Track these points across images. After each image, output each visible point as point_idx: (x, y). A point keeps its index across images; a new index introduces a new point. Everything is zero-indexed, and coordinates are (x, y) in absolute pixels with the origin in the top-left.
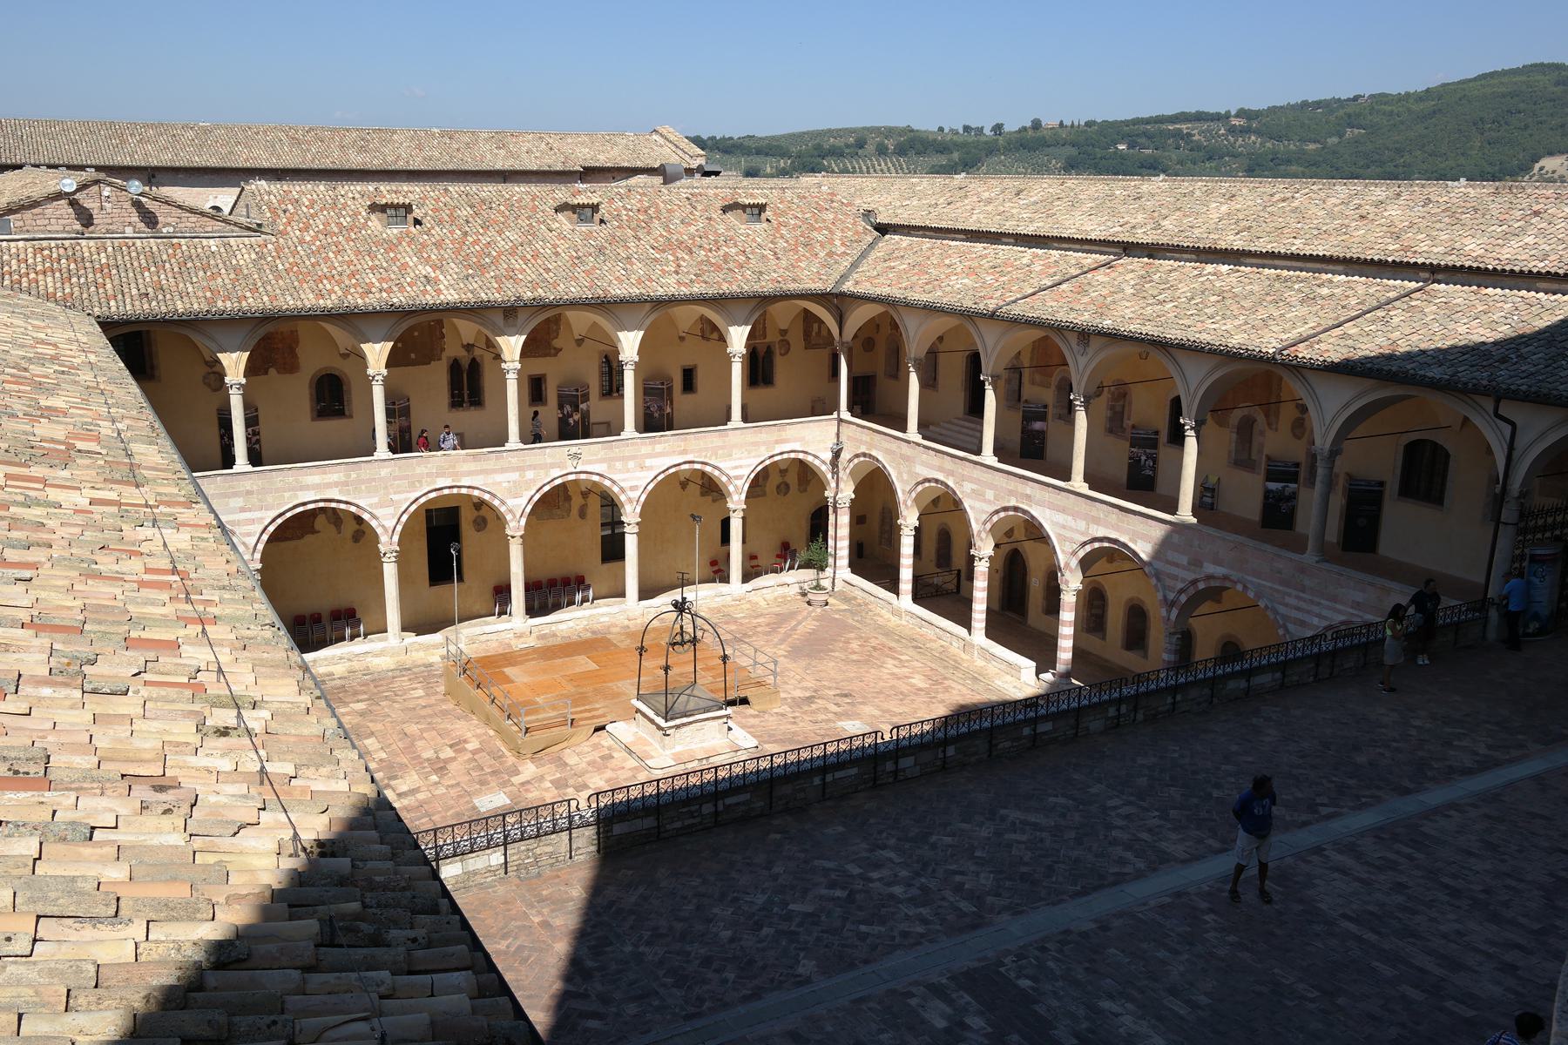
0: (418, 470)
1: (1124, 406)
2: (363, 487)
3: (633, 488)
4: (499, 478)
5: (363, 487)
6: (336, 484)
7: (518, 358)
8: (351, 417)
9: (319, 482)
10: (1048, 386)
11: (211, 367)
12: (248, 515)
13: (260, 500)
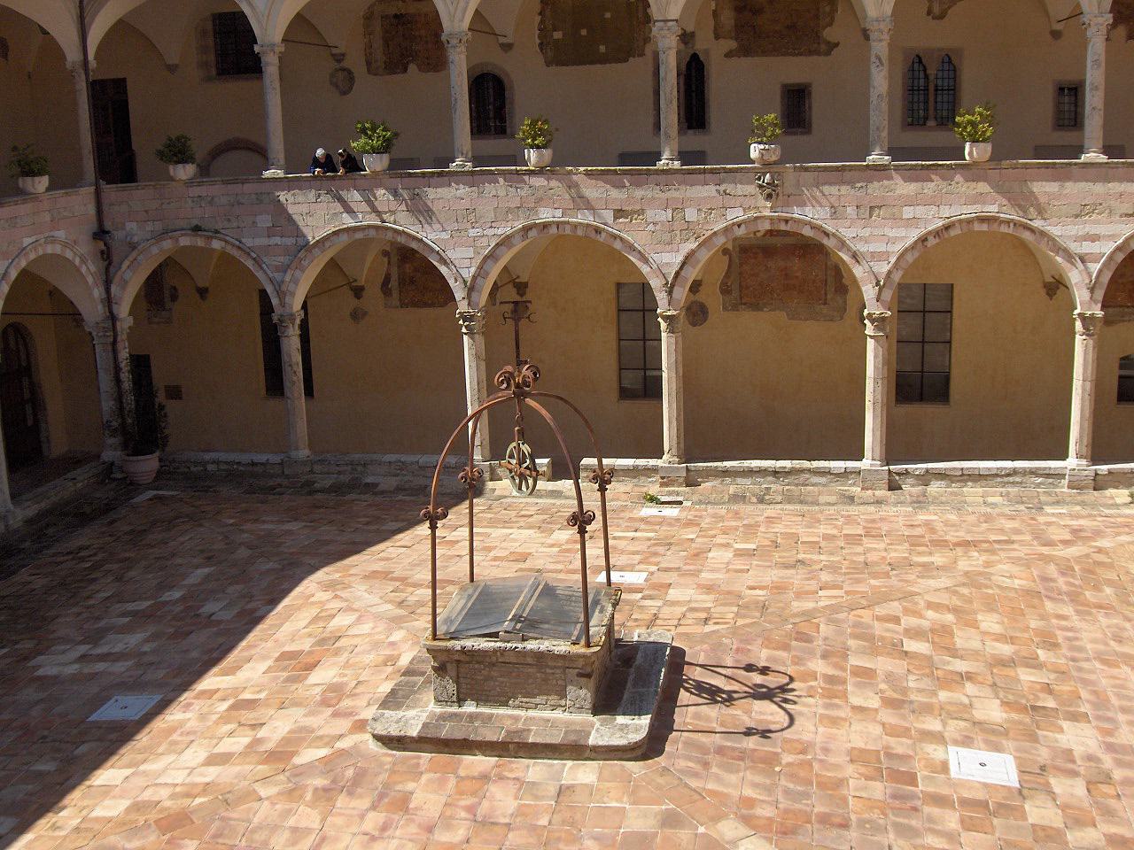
3: (875, 256)
11: (339, 61)
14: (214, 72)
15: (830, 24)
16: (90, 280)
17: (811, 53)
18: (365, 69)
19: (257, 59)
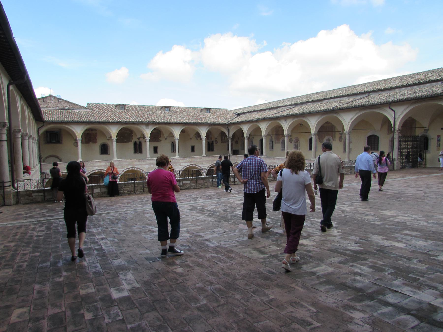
0: (124, 163)
1: (298, 144)
4: (144, 166)
6: (103, 166)
7: (149, 136)
8: (109, 154)
10: (279, 143)
15: (160, 137)
17: (158, 141)
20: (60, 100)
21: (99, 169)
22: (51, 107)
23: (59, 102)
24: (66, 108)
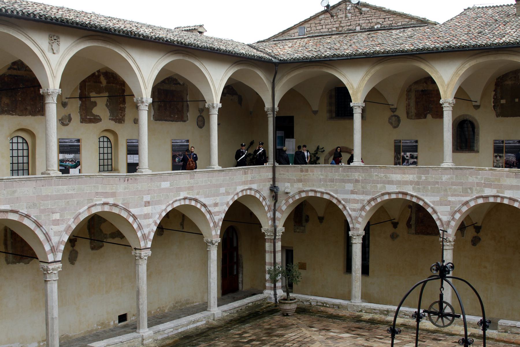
0: (471, 179)
2: (429, 187)
5: (429, 187)
6: (411, 183)
8: (478, 152)
9: (400, 179)
11: (393, 112)
12: (355, 196)
13: (363, 187)
14: (334, 115)
16: (266, 208)
18: (405, 116)
19: (351, 109)
20: (364, 9)
21: (397, 191)
22: (345, 29)
23: (361, 14)
24: (376, 27)
